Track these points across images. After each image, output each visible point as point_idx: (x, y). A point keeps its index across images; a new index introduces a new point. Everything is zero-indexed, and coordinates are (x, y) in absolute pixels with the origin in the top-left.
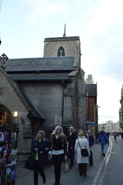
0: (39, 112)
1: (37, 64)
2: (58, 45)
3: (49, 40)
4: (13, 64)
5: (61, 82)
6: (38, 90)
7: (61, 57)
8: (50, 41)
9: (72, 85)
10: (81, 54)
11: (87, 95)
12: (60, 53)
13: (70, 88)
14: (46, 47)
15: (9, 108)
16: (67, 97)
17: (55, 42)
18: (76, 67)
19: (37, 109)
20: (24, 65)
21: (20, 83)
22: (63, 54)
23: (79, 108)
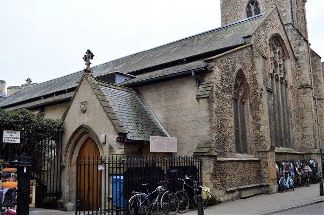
0: (165, 131)
6: (163, 95)
12: (251, 12)
16: (201, 101)
19: (162, 127)
22: (258, 11)
23: (260, 114)
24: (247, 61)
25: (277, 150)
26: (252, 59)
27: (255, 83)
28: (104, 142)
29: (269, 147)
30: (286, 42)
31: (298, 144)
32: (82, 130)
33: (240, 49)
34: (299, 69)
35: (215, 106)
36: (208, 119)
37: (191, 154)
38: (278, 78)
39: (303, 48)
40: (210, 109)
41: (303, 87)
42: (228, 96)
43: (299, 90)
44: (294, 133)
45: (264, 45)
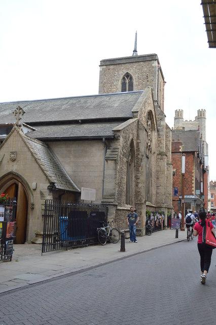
0: (73, 182)
1: (82, 107)
2: (122, 71)
3: (108, 63)
4: (48, 109)
5: (102, 139)
7: (127, 92)
8: (110, 65)
9: (121, 143)
10: (165, 80)
11: (180, 150)
12: (126, 84)
13: (114, 149)
14: (102, 75)
15: (26, 179)
16: (109, 161)
17: (117, 65)
18: (136, 112)
19: (70, 179)
20: (64, 110)
21: (47, 142)
24: (135, 132)
25: (147, 203)
26: (138, 131)
27: (138, 149)
28: (35, 188)
29: (144, 200)
30: (154, 117)
31: (154, 198)
32: (10, 176)
33: (133, 123)
34: (159, 139)
35: (118, 167)
36: (114, 177)
37: (99, 202)
38: (149, 148)
39: (162, 123)
40: (116, 169)
41: (161, 154)
42: (125, 160)
43: (158, 156)
44: (153, 191)
45: (143, 117)
